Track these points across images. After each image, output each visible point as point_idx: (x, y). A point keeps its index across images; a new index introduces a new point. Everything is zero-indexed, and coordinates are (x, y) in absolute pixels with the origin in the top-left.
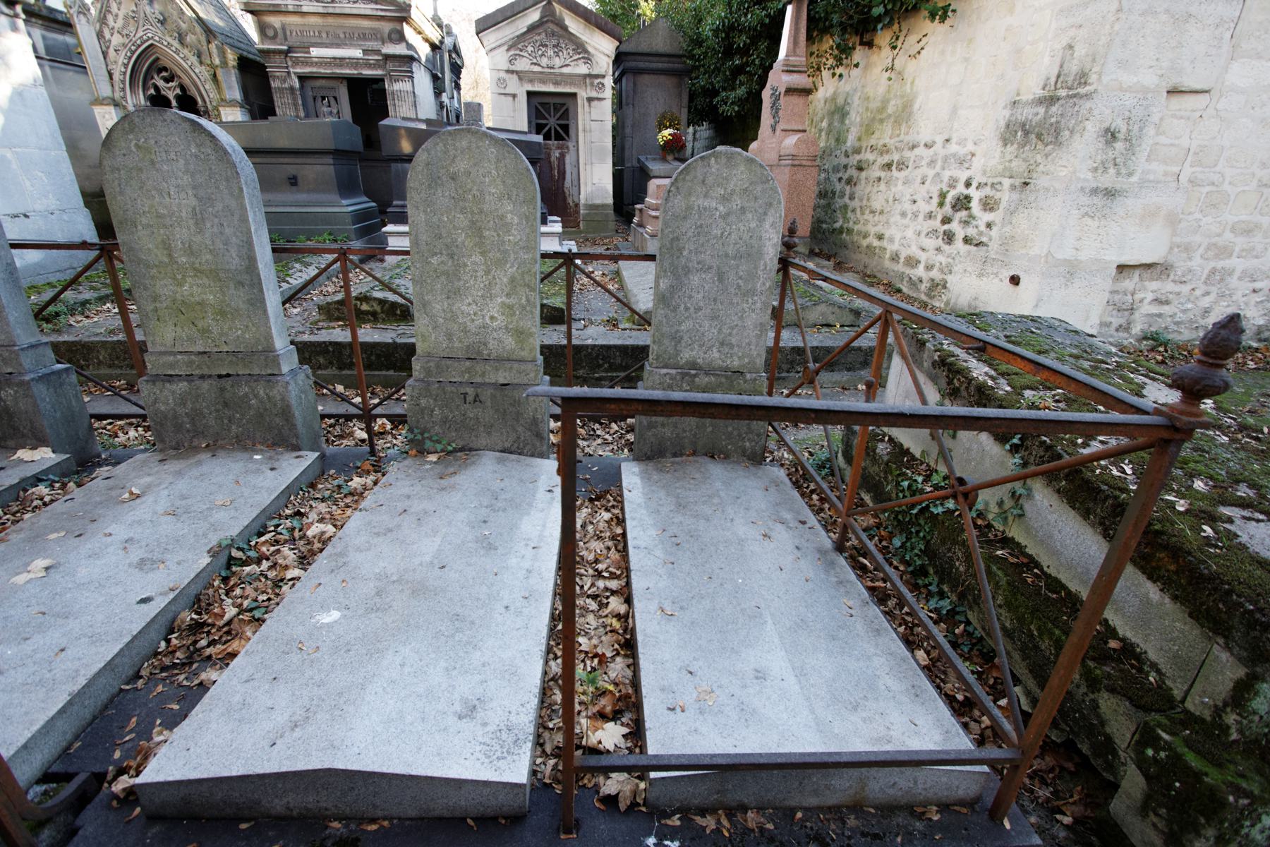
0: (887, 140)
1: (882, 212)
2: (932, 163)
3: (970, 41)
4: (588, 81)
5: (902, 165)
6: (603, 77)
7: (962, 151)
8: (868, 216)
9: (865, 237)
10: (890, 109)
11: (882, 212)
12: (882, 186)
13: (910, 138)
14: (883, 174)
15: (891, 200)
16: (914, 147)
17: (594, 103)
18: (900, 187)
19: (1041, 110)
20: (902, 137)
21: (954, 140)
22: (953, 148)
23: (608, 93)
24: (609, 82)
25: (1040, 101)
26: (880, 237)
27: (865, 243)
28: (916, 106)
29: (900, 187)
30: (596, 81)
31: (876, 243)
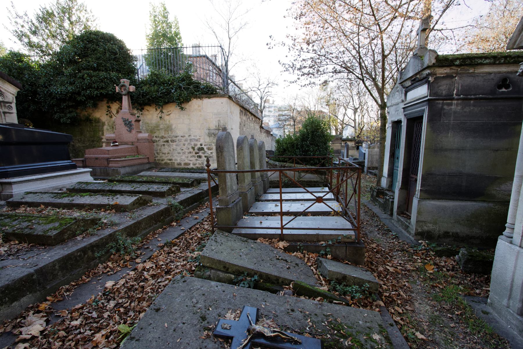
0: (163, 135)
1: (168, 153)
2: (186, 140)
3: (189, 115)
4: (2, 104)
5: (173, 141)
6: (11, 103)
7: (196, 138)
8: (161, 155)
9: (162, 160)
10: (161, 126)
11: (168, 153)
12: (166, 147)
13: (174, 134)
14: (165, 144)
15: (172, 150)
16: (176, 137)
17: (7, 115)
18: (174, 147)
19: (217, 131)
20: (170, 134)
21: (192, 135)
22: (192, 137)
23: (14, 110)
24: (14, 105)
25: (216, 129)
26: (170, 160)
27: (163, 162)
28: (173, 127)
29: (174, 147)
30: (7, 105)
31: (169, 162)
